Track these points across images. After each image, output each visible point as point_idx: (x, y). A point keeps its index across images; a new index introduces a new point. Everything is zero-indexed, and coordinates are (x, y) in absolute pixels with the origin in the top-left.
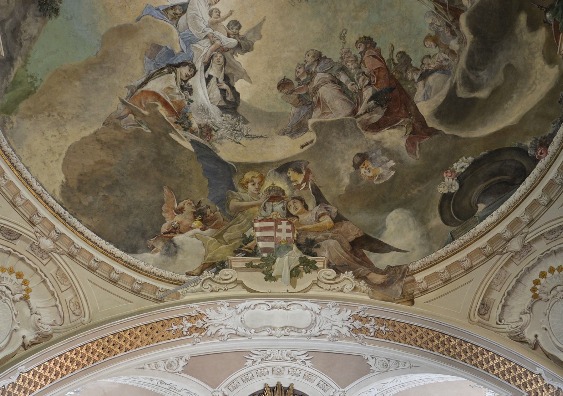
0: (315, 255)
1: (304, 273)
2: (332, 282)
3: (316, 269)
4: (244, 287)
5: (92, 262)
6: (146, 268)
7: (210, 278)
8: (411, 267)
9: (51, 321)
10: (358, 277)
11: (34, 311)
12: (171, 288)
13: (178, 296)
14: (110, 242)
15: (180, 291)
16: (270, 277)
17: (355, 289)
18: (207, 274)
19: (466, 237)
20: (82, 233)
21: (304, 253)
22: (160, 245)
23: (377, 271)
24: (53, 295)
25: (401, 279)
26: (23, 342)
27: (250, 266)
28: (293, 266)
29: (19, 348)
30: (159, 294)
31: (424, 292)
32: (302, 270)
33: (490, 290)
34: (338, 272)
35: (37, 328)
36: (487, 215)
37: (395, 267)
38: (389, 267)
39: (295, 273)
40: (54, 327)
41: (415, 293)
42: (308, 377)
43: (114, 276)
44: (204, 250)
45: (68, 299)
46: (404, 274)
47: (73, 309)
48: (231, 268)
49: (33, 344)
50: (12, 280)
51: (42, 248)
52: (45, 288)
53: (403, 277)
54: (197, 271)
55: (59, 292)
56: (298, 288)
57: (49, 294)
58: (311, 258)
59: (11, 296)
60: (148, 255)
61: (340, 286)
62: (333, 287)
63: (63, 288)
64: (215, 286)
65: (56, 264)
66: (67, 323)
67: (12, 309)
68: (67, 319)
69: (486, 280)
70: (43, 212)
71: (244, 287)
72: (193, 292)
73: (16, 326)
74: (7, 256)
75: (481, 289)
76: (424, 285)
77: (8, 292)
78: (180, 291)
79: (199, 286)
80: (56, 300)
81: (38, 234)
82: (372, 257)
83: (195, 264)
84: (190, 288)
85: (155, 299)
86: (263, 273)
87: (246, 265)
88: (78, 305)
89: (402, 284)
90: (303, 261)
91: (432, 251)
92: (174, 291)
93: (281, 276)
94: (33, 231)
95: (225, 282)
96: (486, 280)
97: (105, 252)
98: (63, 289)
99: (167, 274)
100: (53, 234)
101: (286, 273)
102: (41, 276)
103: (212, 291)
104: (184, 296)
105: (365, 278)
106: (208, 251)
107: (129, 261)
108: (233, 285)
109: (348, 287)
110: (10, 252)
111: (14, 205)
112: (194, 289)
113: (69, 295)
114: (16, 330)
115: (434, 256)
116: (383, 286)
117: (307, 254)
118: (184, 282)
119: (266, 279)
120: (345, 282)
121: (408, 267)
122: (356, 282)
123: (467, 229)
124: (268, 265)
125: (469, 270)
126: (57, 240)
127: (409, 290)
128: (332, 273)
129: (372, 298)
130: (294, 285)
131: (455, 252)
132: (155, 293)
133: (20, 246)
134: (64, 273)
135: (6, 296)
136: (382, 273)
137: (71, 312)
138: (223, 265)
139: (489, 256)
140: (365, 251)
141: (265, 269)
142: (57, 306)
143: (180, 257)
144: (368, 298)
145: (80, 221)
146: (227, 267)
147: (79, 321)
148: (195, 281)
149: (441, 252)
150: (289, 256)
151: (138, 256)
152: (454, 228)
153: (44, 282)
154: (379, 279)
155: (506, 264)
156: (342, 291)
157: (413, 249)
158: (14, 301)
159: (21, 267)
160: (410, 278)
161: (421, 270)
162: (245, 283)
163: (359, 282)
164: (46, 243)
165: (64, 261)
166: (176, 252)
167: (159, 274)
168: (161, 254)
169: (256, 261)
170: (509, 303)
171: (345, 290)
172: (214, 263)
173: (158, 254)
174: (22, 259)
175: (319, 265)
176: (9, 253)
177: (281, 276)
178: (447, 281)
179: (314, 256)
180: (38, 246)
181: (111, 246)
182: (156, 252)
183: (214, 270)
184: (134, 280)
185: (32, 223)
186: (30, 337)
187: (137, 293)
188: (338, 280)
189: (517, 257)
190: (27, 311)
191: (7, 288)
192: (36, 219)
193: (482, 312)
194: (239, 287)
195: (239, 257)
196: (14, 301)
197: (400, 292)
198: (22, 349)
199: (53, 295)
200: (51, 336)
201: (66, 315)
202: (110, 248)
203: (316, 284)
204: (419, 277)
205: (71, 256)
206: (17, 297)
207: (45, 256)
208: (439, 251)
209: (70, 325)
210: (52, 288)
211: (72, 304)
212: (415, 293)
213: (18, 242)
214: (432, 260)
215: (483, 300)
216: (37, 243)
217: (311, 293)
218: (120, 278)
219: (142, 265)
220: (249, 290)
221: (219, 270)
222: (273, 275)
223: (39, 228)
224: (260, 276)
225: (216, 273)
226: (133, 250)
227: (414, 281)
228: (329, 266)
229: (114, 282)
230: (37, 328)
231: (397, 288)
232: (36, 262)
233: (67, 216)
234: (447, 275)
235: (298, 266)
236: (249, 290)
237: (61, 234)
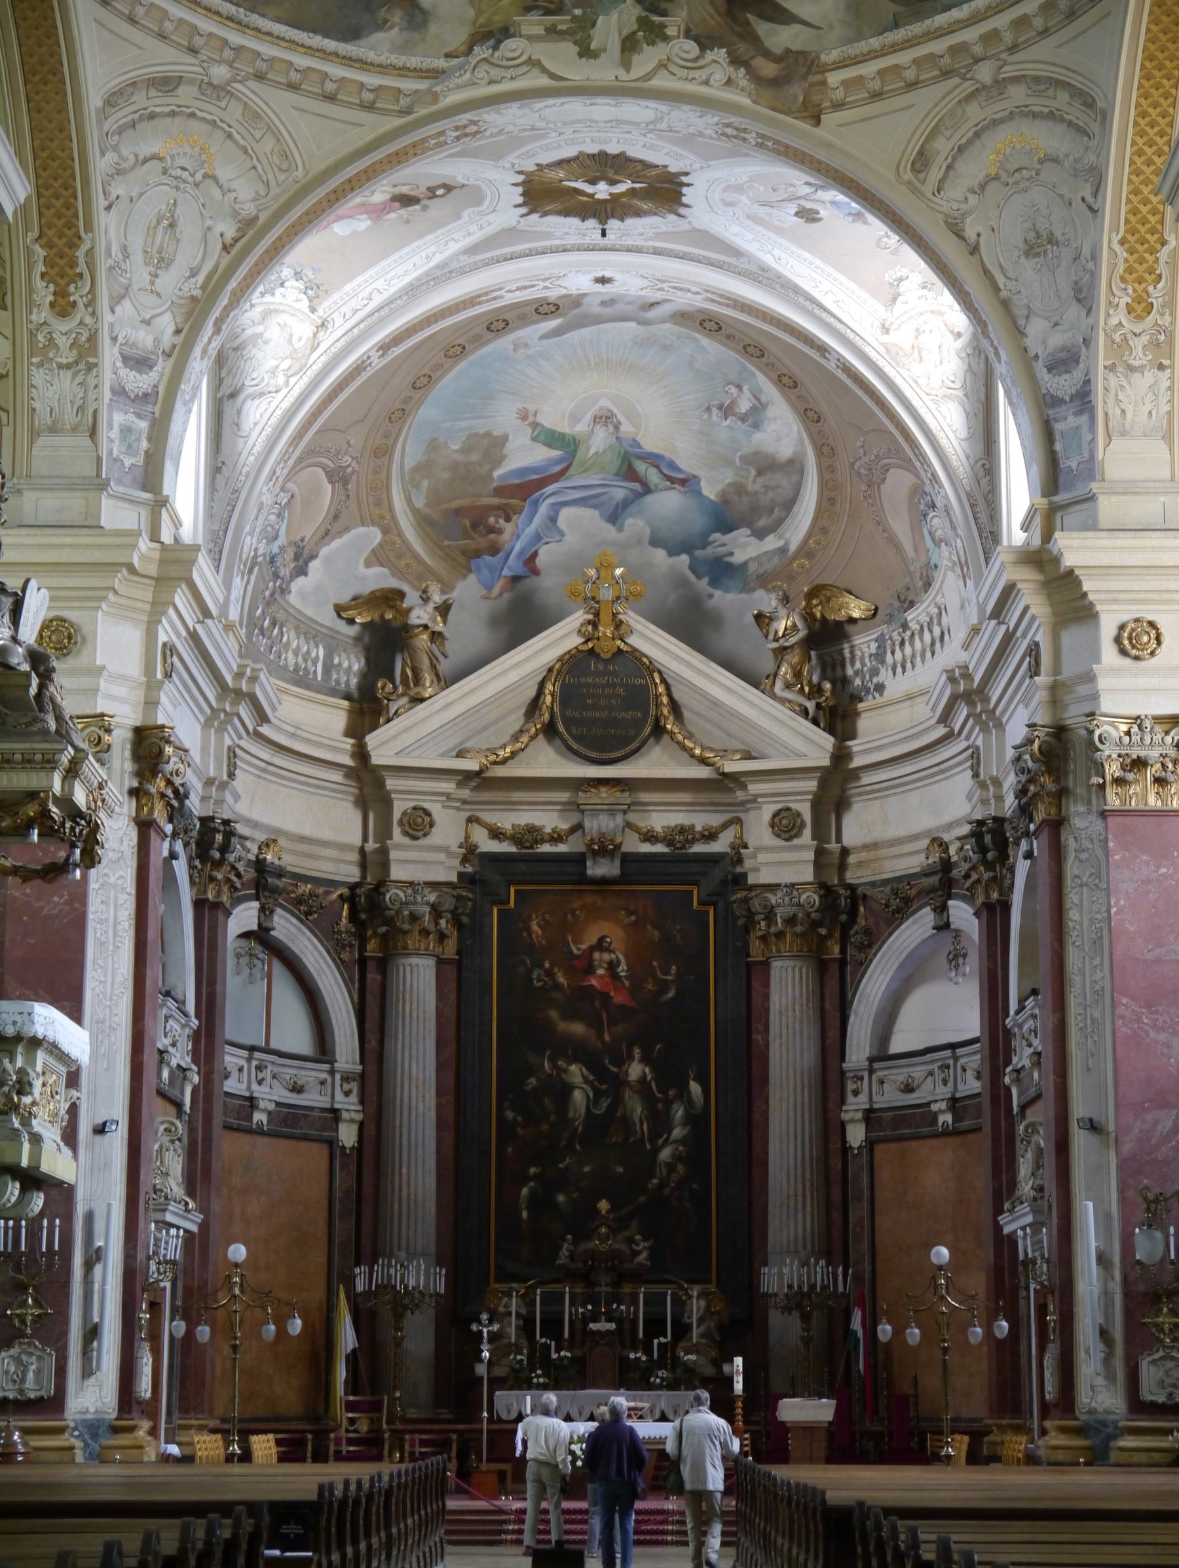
0: (664, 13)
1: (645, 46)
2: (693, 65)
3: (666, 39)
4: (544, 70)
5: (293, 74)
6: (378, 60)
7: (485, 59)
8: (824, 58)
9: (252, 195)
10: (736, 61)
11: (225, 187)
12: (422, 85)
13: (435, 98)
14: (315, 32)
15: (438, 89)
16: (587, 52)
17: (729, 82)
18: (481, 52)
19: (917, 28)
20: (269, 34)
21: (646, 9)
22: (397, 16)
23: (767, 54)
24: (246, 152)
25: (805, 77)
26: (223, 244)
27: (552, 31)
28: (626, 32)
29: (220, 256)
30: (404, 102)
31: (838, 106)
32: (641, 39)
33: (935, 132)
34: (703, 48)
35: (235, 213)
36: (955, 6)
37: (797, 52)
38: (788, 51)
39: (629, 45)
40: (258, 203)
41: (825, 105)
42: (652, 147)
43: (330, 87)
44: (472, 11)
45: (268, 149)
46: (810, 67)
47: (278, 163)
48: (520, 36)
49: (236, 240)
50: (185, 154)
51: (215, 82)
52: (233, 145)
53: (808, 73)
54: (463, 48)
55: (254, 144)
56: (636, 72)
57: (240, 153)
58: (656, 19)
59: (190, 179)
60: (379, 36)
61: (703, 74)
62: (693, 74)
63: (258, 134)
64: (495, 73)
65: (239, 99)
66: (275, 190)
67: (196, 198)
68: (272, 183)
69: (934, 113)
70: (206, 25)
71: (544, 70)
72: (459, 87)
73: (209, 223)
74: (169, 120)
75: (924, 125)
76: (839, 95)
77: (185, 175)
78: (438, 89)
79: (468, 75)
80: (251, 158)
81: (205, 65)
82: (762, 28)
83: (458, 37)
84: (454, 82)
85: (400, 112)
86: (575, 43)
87: (547, 29)
88: (285, 155)
89: (805, 85)
90: (643, 23)
91: (859, 36)
92: (429, 91)
93: (605, 50)
94: (196, 62)
95: (511, 64)
96: (934, 113)
97: (311, 51)
98: (258, 136)
99: (414, 62)
100: (228, 54)
101: (614, 45)
102: (223, 129)
103: (491, 82)
104: (445, 97)
105: (746, 64)
106: (479, 13)
107: (349, 54)
108: (524, 69)
109: (717, 76)
110: (173, 111)
111: (162, 36)
112: (460, 81)
113: (269, 144)
114: (209, 229)
115: (862, 46)
116: (775, 83)
117: (652, 11)
118: (443, 72)
119: (581, 55)
120: (713, 68)
121: (818, 57)
122: (732, 69)
123: (919, 16)
124: (583, 29)
125: (912, 85)
126: (234, 61)
127: (816, 98)
128: (692, 47)
129: (755, 102)
130: (626, 65)
131: (895, 48)
132: (398, 101)
133: (186, 95)
134: (255, 112)
135: (185, 182)
136: (776, 59)
137: (276, 169)
138: (505, 32)
139: (946, 74)
140: (750, 17)
141: (578, 37)
142: (254, 168)
143: (433, 28)
144: (746, 101)
145: (263, 15)
146: (513, 36)
147: (291, 179)
148: (461, 67)
149: (875, 42)
150: (621, 13)
151: (363, 42)
152: (899, 9)
153: (230, 136)
154: (769, 69)
155: (969, 98)
156: (706, 83)
157: (831, 27)
158: (197, 185)
159: (195, 125)
160: (819, 77)
161: (839, 65)
162: (545, 62)
163: (737, 70)
164: (220, 73)
165: (250, 90)
166: (425, 23)
167: (401, 64)
168: (401, 30)
169: (562, 22)
170: (957, 165)
171: (712, 82)
172: (491, 32)
173: (394, 32)
174: (192, 115)
175: (671, 31)
176: (173, 114)
177: (605, 50)
178: (876, 96)
179: (662, 15)
180: (210, 84)
181: (319, 38)
182: (392, 27)
183: (491, 42)
184: (362, 85)
185: (193, 51)
186: (230, 233)
187: (369, 107)
188: (701, 63)
189: (984, 93)
190: (216, 193)
191: (183, 169)
192: (198, 41)
193: (918, 165)
194: (536, 71)
195: (534, 17)
196: (197, 185)
197: (801, 99)
198: (224, 254)
199: (246, 152)
200: (256, 218)
201: (271, 177)
202: (317, 41)
203: (665, 66)
204: (834, 78)
205: (260, 77)
206: (199, 176)
207: (222, 94)
208: (871, 40)
209: (278, 190)
210: (242, 142)
211: (275, 157)
212: (825, 105)
213: (181, 90)
214: (858, 52)
215: (923, 145)
216: (206, 79)
217: (656, 82)
218: (339, 89)
219: (371, 56)
220: (553, 76)
221: (499, 42)
222: (593, 46)
223: (205, 54)
224: (569, 48)
225: (495, 48)
226: (353, 34)
227: (824, 83)
228: (688, 34)
229: (331, 98)
230: (235, 213)
231: (797, 91)
232: (210, 110)
233: (242, 16)
234: (876, 85)
235: (634, 33)
236: (553, 76)
237: (238, 49)
